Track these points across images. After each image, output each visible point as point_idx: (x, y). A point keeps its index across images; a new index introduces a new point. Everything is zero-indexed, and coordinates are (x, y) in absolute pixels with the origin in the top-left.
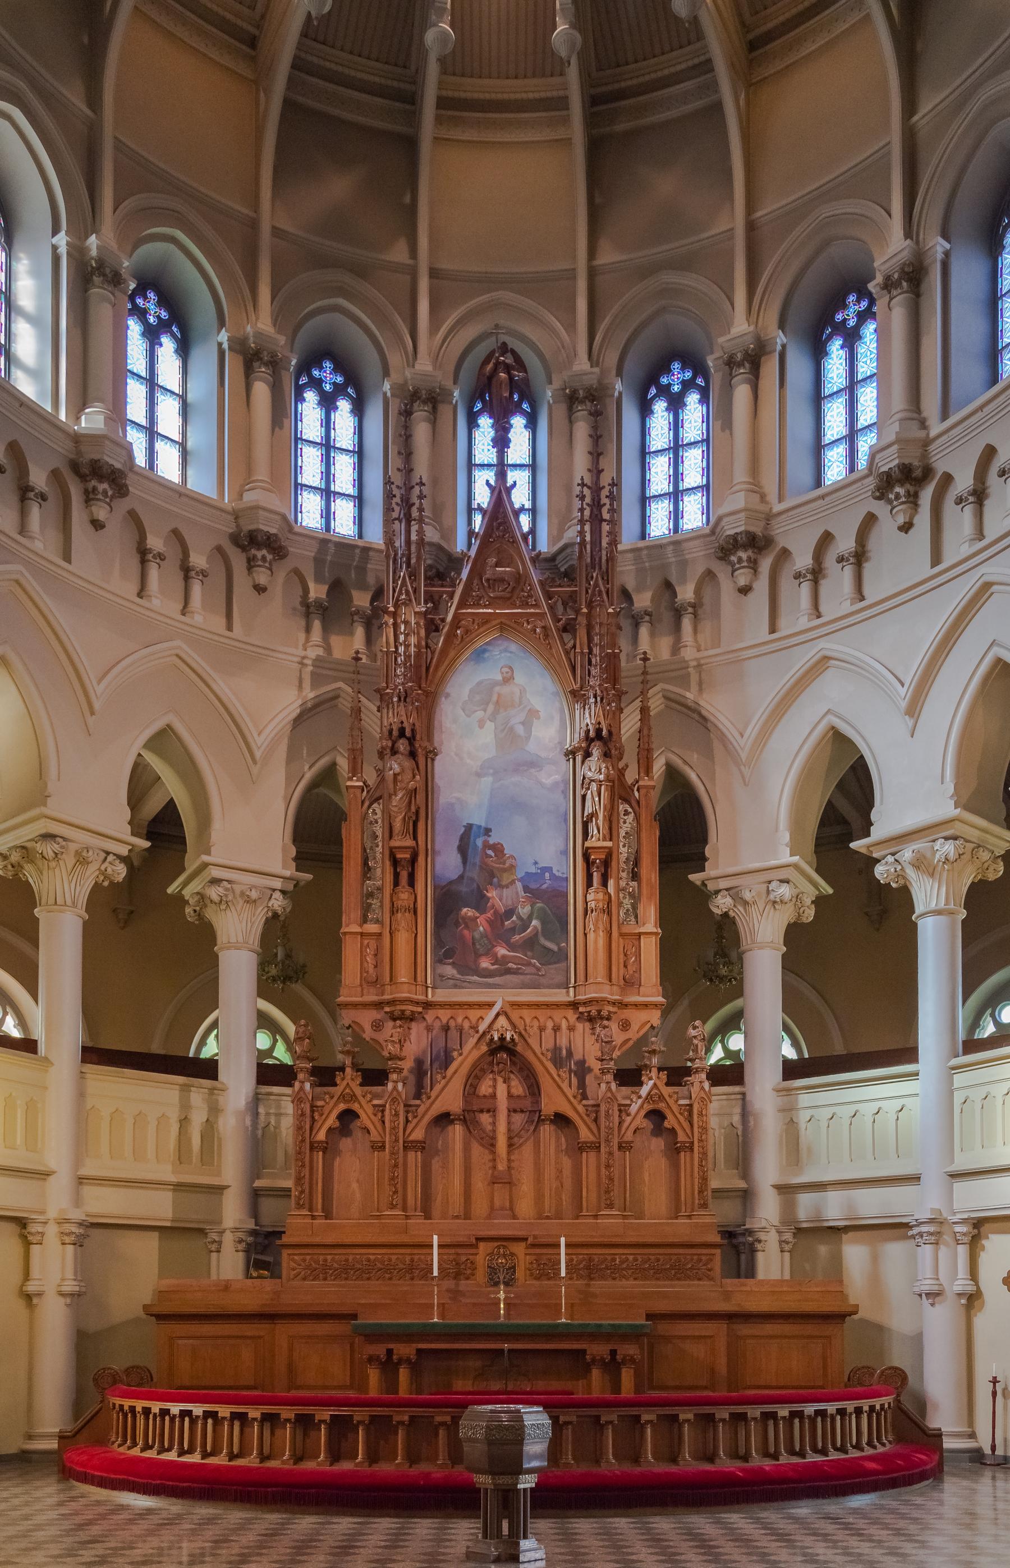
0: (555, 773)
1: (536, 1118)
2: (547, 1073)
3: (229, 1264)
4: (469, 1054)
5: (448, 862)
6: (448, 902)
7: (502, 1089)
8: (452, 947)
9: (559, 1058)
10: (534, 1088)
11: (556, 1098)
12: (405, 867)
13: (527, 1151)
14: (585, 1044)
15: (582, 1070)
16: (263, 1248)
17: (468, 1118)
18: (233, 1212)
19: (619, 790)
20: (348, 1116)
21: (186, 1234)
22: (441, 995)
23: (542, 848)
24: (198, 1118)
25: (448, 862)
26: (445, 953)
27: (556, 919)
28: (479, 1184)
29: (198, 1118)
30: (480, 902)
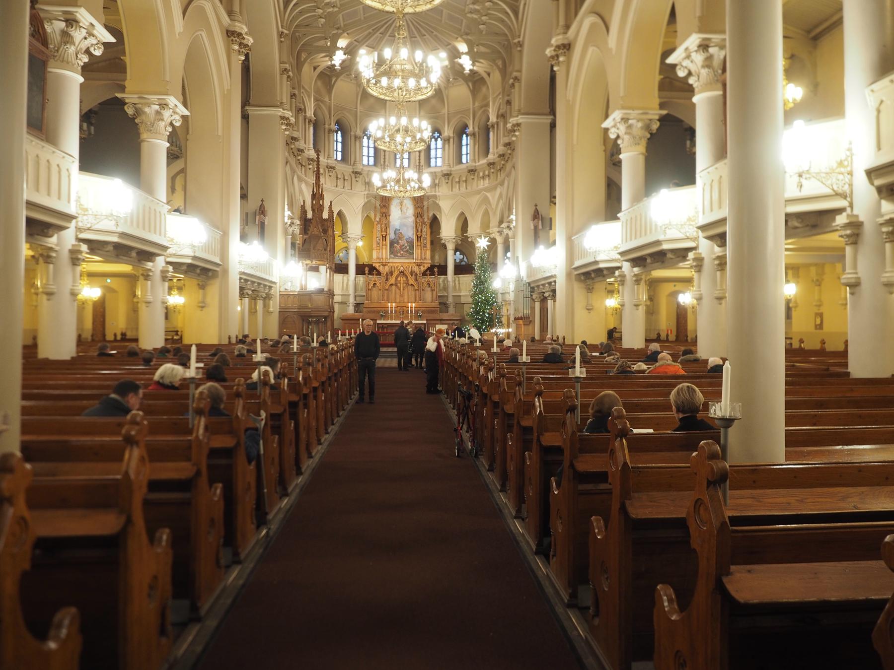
0: (411, 219)
1: (408, 284)
2: (409, 277)
3: (351, 310)
4: (396, 273)
5: (392, 236)
6: (392, 243)
7: (401, 279)
8: (393, 252)
9: (412, 273)
10: (407, 279)
11: (411, 281)
12: (384, 238)
13: (406, 292)
14: (416, 269)
15: (416, 275)
16: (357, 306)
17: (396, 284)
18: (352, 300)
19: (423, 223)
20: (375, 284)
21: (343, 303)
22: (391, 260)
23: (409, 233)
24: (345, 282)
25: (392, 236)
26: (392, 252)
27: (412, 247)
28: (398, 296)
29: (345, 282)
30: (398, 243)
